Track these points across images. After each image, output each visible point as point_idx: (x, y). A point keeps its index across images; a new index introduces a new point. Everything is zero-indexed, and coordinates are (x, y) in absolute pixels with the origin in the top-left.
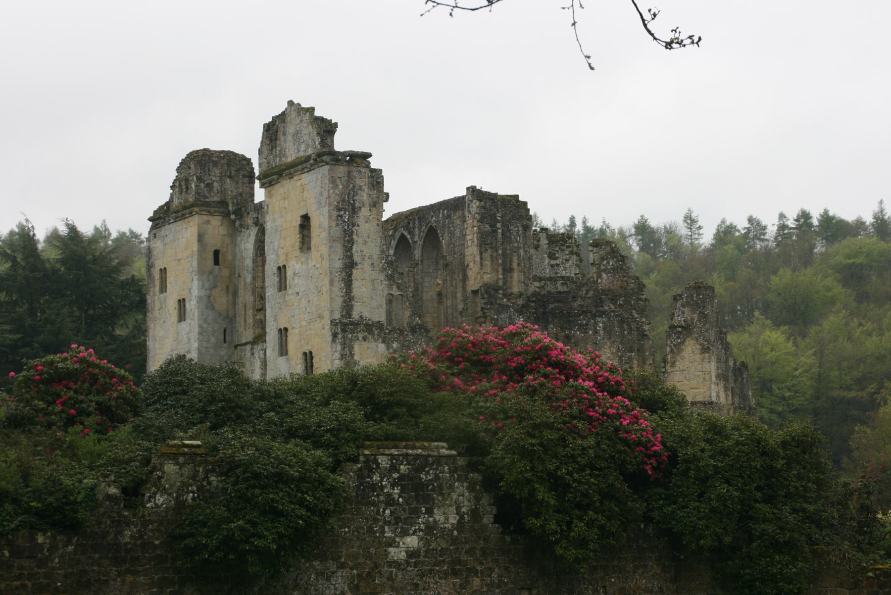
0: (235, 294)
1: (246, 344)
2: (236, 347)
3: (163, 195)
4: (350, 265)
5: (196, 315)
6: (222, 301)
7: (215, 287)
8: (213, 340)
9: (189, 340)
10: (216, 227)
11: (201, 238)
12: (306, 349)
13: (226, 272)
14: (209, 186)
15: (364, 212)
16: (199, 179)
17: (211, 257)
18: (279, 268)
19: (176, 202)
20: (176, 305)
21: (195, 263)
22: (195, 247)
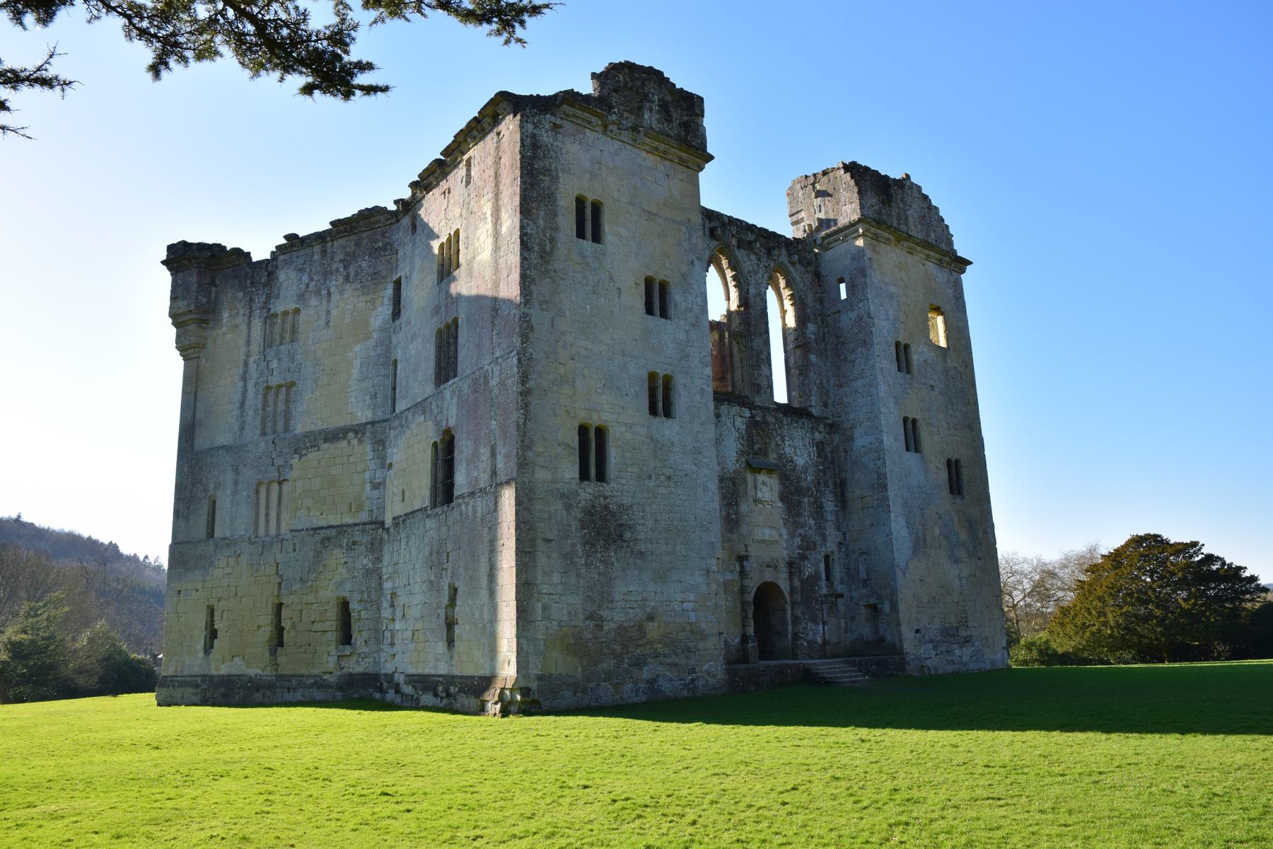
9: (686, 357)
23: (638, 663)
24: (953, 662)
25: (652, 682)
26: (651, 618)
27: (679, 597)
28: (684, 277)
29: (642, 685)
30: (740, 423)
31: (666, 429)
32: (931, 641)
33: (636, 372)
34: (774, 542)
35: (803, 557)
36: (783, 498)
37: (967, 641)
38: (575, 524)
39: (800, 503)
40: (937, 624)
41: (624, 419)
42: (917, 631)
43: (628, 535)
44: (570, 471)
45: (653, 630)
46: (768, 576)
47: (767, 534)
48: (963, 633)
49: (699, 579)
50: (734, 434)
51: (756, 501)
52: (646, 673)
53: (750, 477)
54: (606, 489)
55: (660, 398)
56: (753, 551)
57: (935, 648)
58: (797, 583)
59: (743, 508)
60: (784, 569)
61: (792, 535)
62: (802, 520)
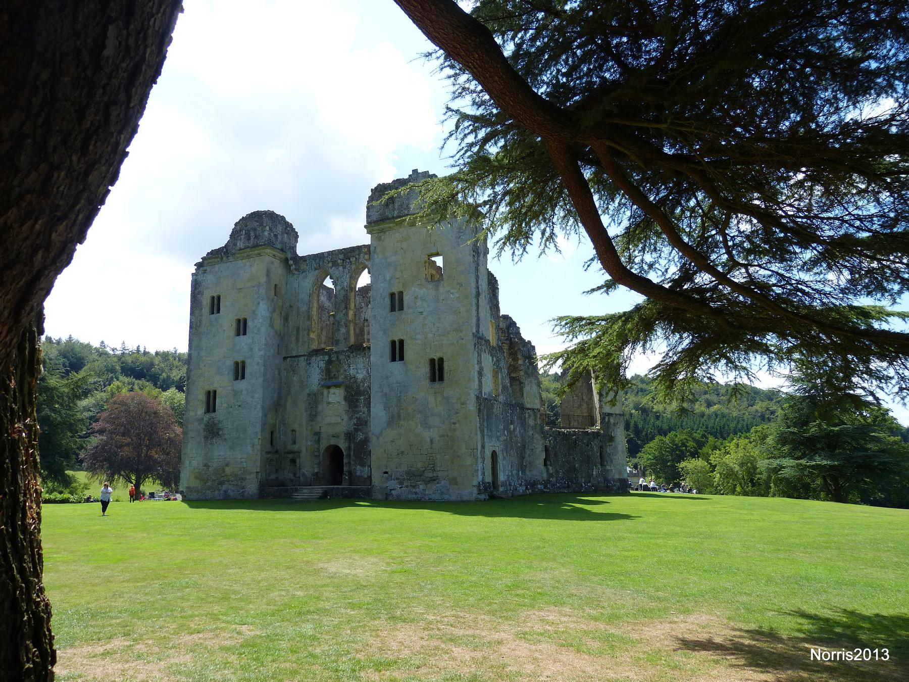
0: (286, 319)
1: (300, 356)
2: (285, 358)
3: (222, 240)
4: (478, 294)
5: (263, 330)
6: (278, 322)
7: (274, 311)
8: (272, 351)
9: (251, 350)
10: (278, 269)
11: (268, 273)
12: (436, 356)
13: (280, 302)
14: (276, 236)
15: (482, 255)
16: (270, 229)
17: (273, 288)
18: (392, 295)
19: (240, 244)
20: (234, 324)
21: (263, 291)
22: (264, 279)
23: (221, 483)
24: (416, 493)
25: (226, 492)
26: (227, 465)
27: (239, 456)
28: (254, 312)
29: (222, 492)
30: (322, 364)
31: (242, 385)
32: (397, 479)
33: (230, 363)
34: (338, 423)
35: (356, 430)
36: (345, 399)
37: (433, 480)
38: (202, 430)
39: (357, 400)
40: (404, 468)
41: (223, 384)
42: (386, 473)
43: (220, 433)
44: (201, 411)
45: (228, 470)
46: (333, 442)
47: (333, 420)
48: (429, 474)
49: (249, 448)
50: (318, 371)
51: (329, 403)
52: (224, 488)
53: (325, 391)
54: (213, 415)
55: (239, 371)
56: (323, 430)
57: (401, 483)
58: (352, 446)
59: (320, 407)
60: (342, 436)
61: (350, 419)
62: (358, 409)
